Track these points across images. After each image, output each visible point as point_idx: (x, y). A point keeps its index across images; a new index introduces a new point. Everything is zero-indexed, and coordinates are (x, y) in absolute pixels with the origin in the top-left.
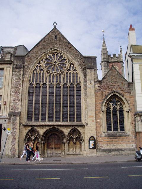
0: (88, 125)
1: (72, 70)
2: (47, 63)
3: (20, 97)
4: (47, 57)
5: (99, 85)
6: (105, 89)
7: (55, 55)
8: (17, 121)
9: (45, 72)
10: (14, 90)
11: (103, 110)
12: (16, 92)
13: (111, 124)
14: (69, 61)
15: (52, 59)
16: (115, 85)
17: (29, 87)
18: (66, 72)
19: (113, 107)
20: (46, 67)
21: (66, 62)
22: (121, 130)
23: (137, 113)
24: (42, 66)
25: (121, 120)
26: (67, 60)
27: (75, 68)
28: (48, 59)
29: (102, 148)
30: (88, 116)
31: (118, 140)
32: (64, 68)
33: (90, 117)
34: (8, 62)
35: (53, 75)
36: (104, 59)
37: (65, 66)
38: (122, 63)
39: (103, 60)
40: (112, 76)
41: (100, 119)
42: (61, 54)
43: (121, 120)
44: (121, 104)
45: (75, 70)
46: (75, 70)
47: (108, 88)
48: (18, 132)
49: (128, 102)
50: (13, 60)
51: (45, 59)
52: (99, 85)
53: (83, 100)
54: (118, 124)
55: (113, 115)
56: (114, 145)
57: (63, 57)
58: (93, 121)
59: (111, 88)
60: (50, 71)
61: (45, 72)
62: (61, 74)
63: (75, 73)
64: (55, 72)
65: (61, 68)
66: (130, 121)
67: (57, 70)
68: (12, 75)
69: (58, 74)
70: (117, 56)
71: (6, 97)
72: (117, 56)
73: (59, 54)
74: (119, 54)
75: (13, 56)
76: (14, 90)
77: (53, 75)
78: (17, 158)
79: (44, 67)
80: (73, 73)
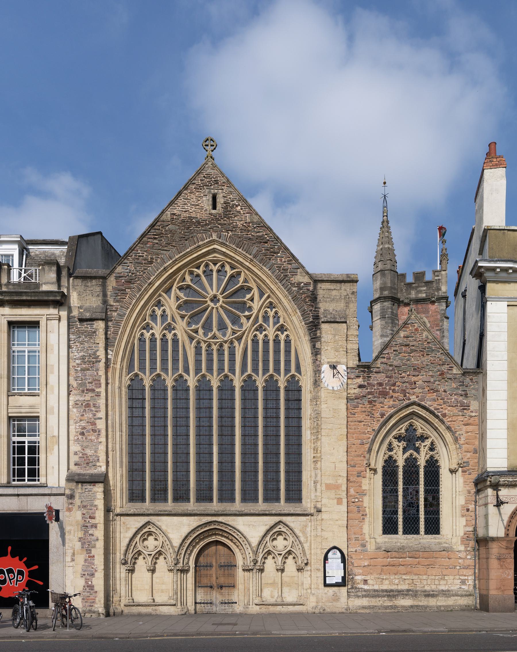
0: (324, 516)
1: (271, 331)
2: (186, 302)
3: (101, 425)
4: (184, 279)
5: (360, 381)
6: (384, 394)
7: (212, 271)
8: (96, 502)
9: (179, 337)
10: (78, 398)
11: (372, 466)
12: (88, 405)
13: (396, 512)
14: (261, 294)
15: (204, 289)
16: (413, 379)
17: (130, 388)
18: (251, 337)
19: (407, 454)
20: (183, 317)
21: (252, 300)
22: (427, 532)
23: (485, 475)
24: (168, 312)
25: (430, 499)
26: (255, 291)
27: (281, 321)
28: (188, 287)
29: (366, 587)
30: (323, 485)
31: (419, 563)
32: (243, 320)
33: (329, 487)
34: (51, 298)
35: (209, 346)
36: (382, 289)
37: (247, 313)
38: (444, 305)
39: (377, 296)
40: (408, 350)
41: (363, 494)
42: (232, 267)
43: (430, 499)
44: (432, 449)
45: (282, 329)
46: (282, 326)
47: (394, 391)
48: (101, 537)
49: (456, 440)
50: (65, 291)
51: (180, 288)
52: (360, 381)
53: (309, 432)
54: (418, 511)
55: (404, 484)
56: (404, 577)
57: (241, 279)
58: (339, 501)
59: (404, 392)
60: (196, 331)
61: (182, 336)
62: (236, 343)
63: (282, 337)
64: (214, 337)
65: (235, 320)
66: (461, 501)
67: (222, 327)
68: (69, 347)
69: (226, 342)
70: (429, 277)
71: (53, 420)
72: (429, 277)
73: (227, 268)
74: (435, 272)
75: (64, 273)
76: (78, 398)
77: (209, 346)
78: (102, 617)
79: (178, 318)
80: (277, 341)
